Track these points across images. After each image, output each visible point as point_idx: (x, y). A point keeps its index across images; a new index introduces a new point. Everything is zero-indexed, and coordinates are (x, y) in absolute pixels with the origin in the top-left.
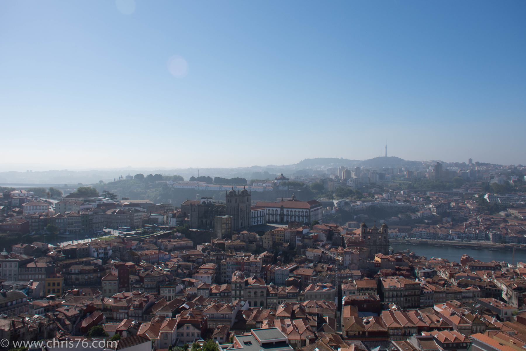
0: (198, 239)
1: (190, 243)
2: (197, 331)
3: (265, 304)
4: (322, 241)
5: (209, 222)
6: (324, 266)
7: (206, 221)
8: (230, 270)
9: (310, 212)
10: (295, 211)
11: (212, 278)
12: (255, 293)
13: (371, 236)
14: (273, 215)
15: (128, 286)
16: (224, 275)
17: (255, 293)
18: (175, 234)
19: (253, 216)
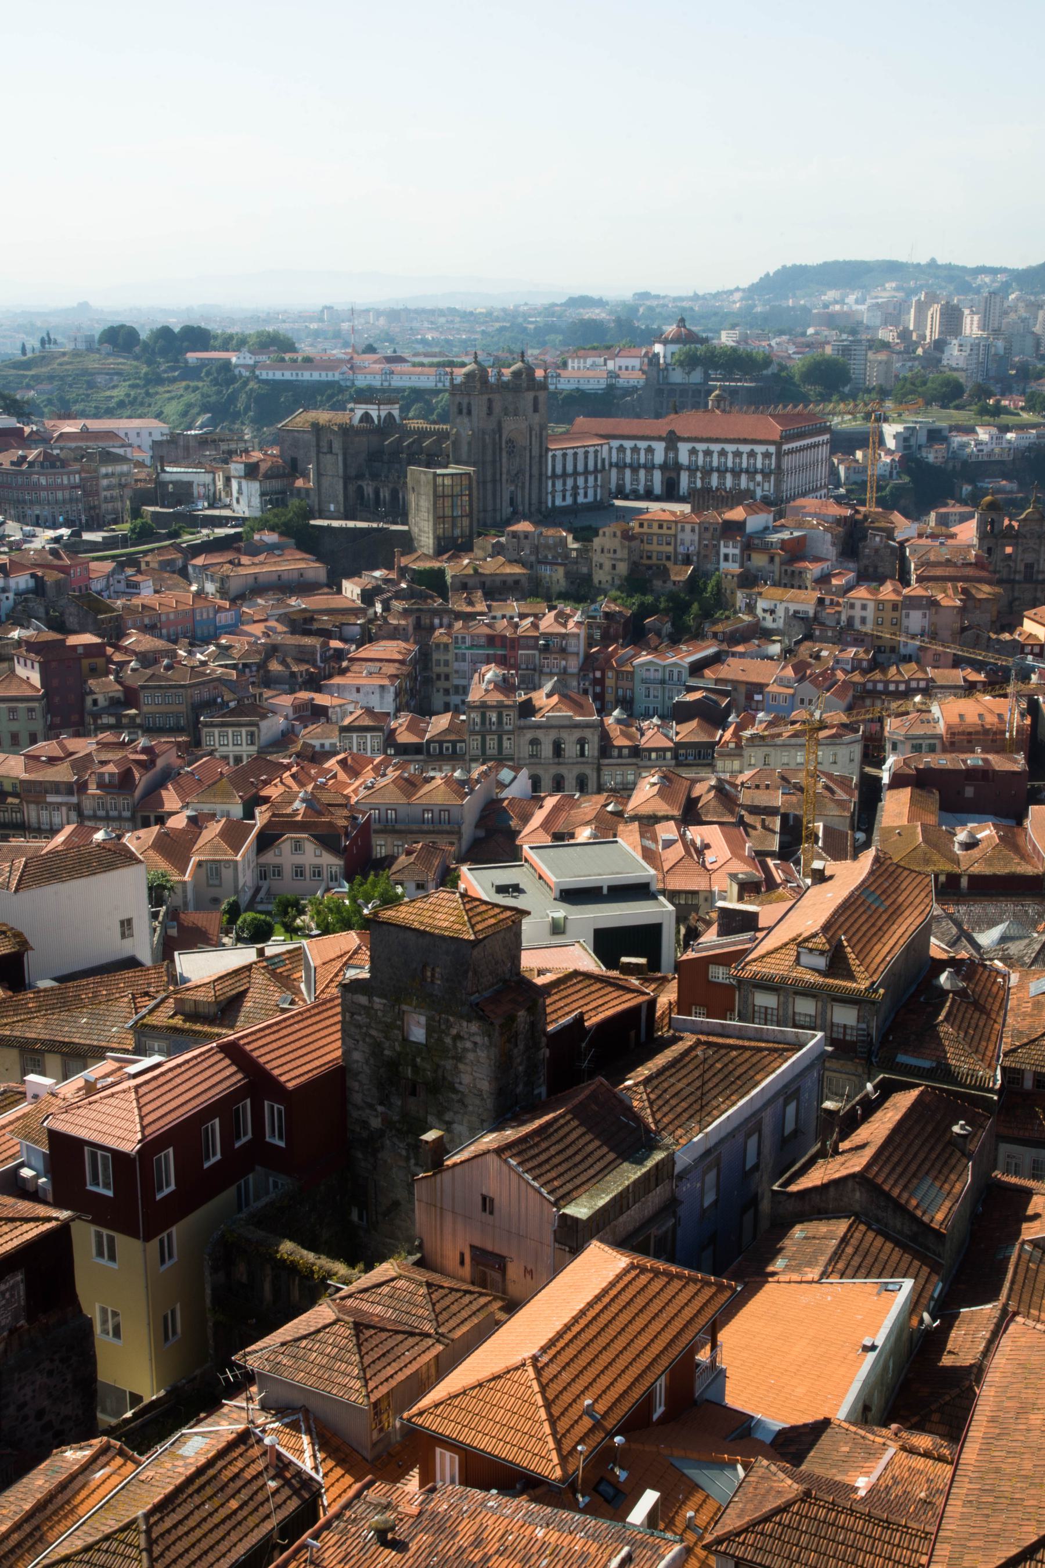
0: (344, 556)
1: (313, 568)
2: (330, 862)
3: (592, 784)
4: (817, 559)
5: (385, 494)
6: (824, 653)
7: (377, 492)
8: (465, 666)
9: (779, 454)
10: (723, 453)
11: (397, 695)
12: (558, 749)
13: (1015, 545)
14: (635, 468)
15: (82, 723)
16: (442, 684)
17: (558, 749)
18: (257, 537)
19: (559, 470)
